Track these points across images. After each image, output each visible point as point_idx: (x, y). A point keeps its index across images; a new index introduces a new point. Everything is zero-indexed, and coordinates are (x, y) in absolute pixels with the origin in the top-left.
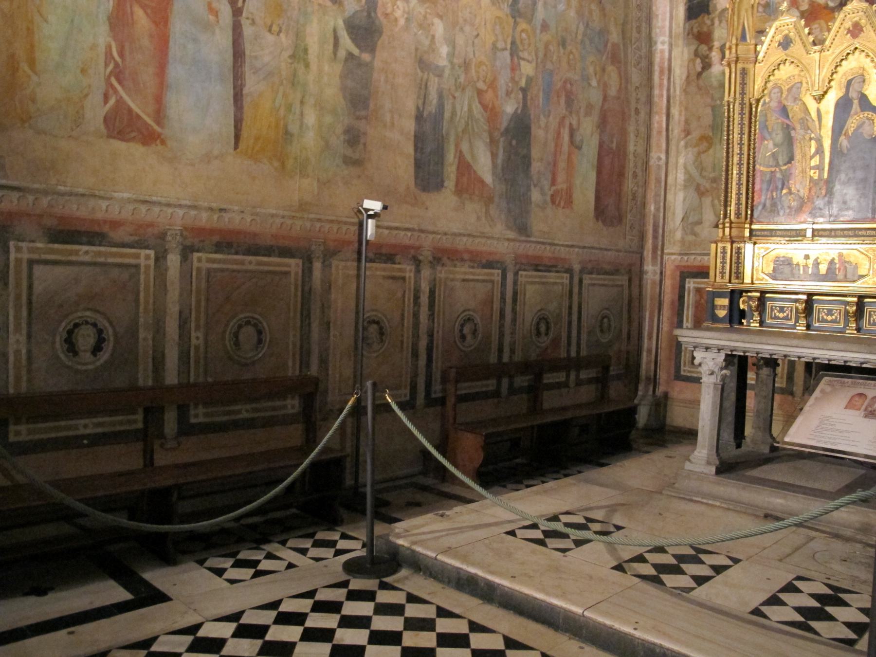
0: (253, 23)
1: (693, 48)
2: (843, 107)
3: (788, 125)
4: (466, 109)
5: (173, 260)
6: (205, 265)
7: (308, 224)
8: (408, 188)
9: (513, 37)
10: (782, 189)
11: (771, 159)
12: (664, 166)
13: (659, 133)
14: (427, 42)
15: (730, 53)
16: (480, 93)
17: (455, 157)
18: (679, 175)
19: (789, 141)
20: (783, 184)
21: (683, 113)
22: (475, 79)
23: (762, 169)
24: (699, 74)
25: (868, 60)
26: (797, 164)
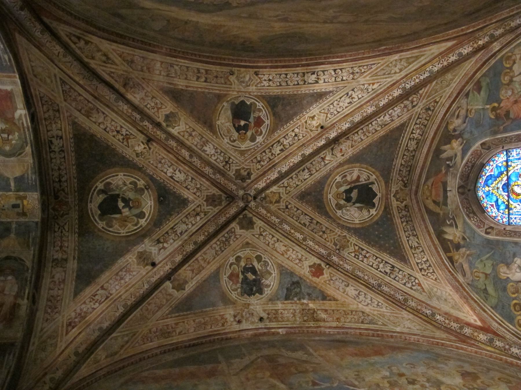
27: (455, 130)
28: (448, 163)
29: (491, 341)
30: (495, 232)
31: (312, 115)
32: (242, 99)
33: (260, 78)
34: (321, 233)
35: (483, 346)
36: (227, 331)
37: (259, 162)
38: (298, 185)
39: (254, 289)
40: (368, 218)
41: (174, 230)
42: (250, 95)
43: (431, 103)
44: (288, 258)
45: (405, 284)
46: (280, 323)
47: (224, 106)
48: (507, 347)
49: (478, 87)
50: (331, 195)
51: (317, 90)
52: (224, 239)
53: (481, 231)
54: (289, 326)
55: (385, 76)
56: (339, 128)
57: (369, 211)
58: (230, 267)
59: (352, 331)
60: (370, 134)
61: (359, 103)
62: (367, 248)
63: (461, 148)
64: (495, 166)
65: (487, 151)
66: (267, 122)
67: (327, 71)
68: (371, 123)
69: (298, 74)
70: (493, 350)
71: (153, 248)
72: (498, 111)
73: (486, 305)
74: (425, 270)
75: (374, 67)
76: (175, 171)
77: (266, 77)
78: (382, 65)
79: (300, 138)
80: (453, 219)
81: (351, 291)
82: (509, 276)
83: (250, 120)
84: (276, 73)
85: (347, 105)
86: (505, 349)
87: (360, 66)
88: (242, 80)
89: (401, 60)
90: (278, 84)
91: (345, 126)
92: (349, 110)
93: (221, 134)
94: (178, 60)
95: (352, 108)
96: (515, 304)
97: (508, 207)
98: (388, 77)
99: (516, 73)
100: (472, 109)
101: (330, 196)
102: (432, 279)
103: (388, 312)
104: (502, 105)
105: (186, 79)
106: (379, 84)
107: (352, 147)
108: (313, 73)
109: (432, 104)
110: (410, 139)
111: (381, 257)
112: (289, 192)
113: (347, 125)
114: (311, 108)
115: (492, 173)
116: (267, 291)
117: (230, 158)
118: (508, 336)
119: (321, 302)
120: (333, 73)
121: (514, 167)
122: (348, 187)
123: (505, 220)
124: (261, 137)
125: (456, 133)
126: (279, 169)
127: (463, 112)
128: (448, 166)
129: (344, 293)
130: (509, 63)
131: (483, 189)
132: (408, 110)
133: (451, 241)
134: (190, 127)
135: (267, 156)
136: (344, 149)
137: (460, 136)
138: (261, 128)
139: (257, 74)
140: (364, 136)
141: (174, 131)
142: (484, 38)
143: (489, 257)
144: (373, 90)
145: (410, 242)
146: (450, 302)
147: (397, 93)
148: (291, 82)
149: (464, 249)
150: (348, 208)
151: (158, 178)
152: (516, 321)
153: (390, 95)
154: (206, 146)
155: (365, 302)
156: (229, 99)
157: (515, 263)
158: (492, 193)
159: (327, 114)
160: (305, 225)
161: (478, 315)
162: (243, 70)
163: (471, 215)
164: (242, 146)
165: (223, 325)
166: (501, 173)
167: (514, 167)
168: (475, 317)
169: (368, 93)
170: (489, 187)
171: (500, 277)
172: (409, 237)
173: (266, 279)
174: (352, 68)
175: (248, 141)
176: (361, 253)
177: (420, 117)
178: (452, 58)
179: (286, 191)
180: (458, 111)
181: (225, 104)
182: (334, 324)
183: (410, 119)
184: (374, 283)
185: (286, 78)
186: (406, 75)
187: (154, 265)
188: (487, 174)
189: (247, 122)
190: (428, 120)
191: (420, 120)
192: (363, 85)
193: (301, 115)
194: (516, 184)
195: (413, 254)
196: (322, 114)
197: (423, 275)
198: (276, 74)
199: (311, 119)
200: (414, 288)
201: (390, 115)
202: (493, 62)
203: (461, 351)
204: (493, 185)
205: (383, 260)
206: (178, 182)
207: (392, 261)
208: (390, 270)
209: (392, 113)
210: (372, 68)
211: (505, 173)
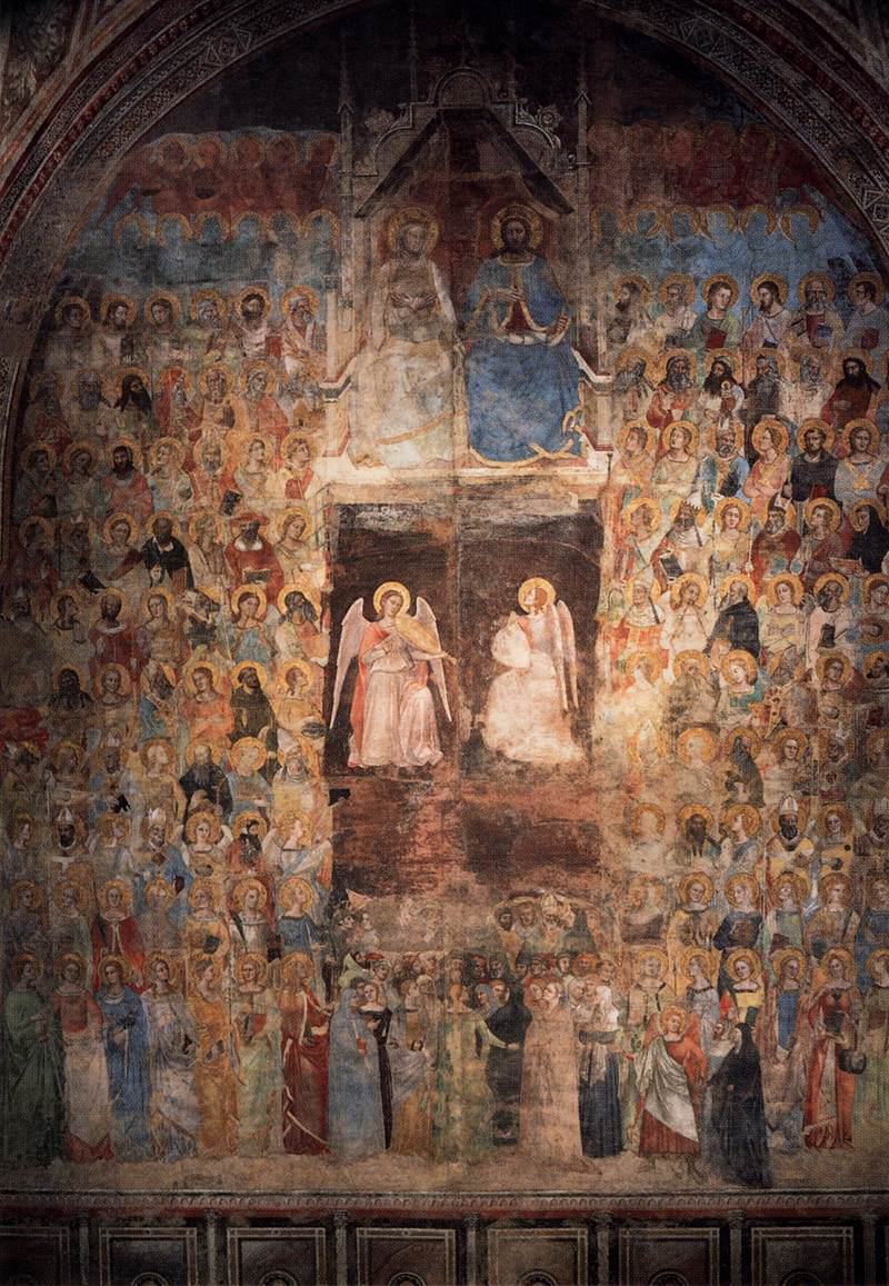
0: (397, 1046)
4: (649, 1066)
5: (341, 1233)
6: (366, 1236)
7: (460, 1201)
8: (574, 1156)
9: (722, 970)
14: (588, 1014)
16: (669, 1046)
17: (636, 1119)
22: (661, 1030)
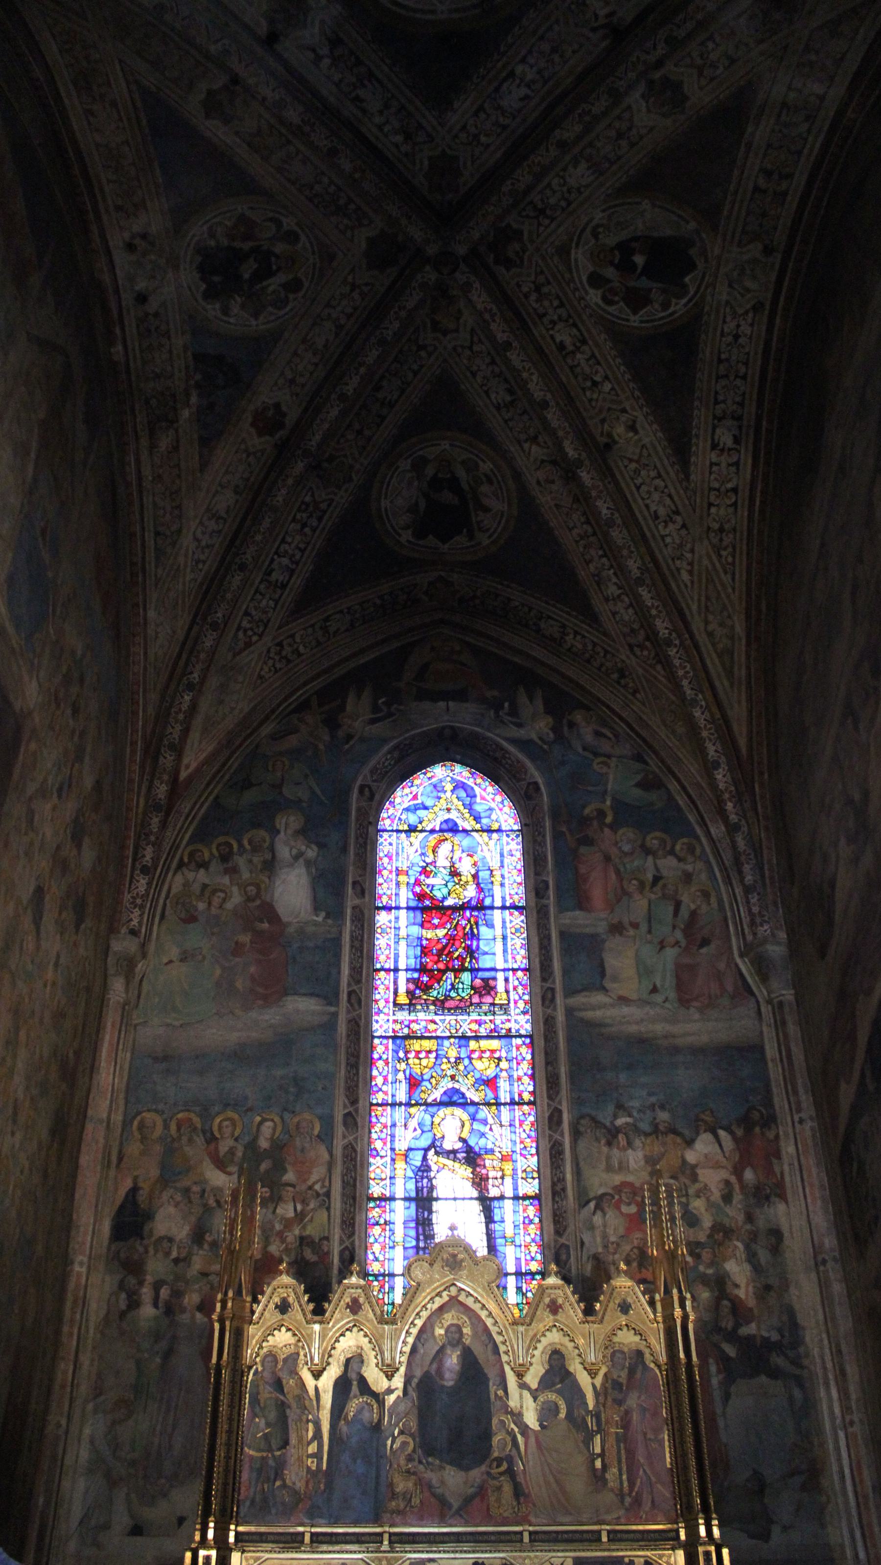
1: (118, 1277)
2: (342, 1386)
3: (283, 1403)
10: (275, 1480)
11: (263, 1443)
12: (63, 1438)
13: (63, 1387)
15: (224, 1307)
18: (81, 1451)
19: (282, 1423)
20: (276, 1474)
21: (96, 1363)
23: (251, 1452)
24: (123, 1315)
25: (367, 1339)
26: (292, 1451)
27: (572, 725)
28: (506, 705)
29: (157, 807)
30: (364, 804)
31: (638, 426)
32: (700, 265)
33: (747, 313)
34: (357, 426)
35: (144, 790)
36: (105, 218)
37: (538, 289)
38: (474, 374)
39: (216, 279)
40: (392, 527)
41: (366, 82)
42: (706, 288)
43: (634, 682)
44: (295, 354)
45: (247, 613)
46: (137, 344)
47: (688, 222)
48: (152, 838)
49: (649, 784)
50: (447, 447)
51: (697, 445)
52: (342, 202)
53: (365, 776)
54: (132, 365)
55: (703, 599)
56: (601, 492)
57: (407, 527)
58: (271, 220)
59: (138, 516)
60: (581, 549)
61: (653, 536)
62: (324, 529)
63: (534, 736)
64: (493, 805)
65: (522, 793)
66: (635, 320)
67: (737, 473)
68: (605, 555)
69: (741, 404)
70: (140, 810)
71: (316, 30)
72: (595, 823)
73: (220, 786)
74: (279, 653)
75: (726, 579)
76: (528, 86)
77: (746, 329)
78: (728, 597)
79: (588, 393)
80: (390, 715)
81: (225, 501)
82: (282, 833)
83: (644, 278)
84: (752, 354)
85: (653, 508)
86: (147, 835)
87: (734, 547)
88: (748, 272)
89: (732, 638)
90: (723, 356)
91: (604, 508)
92: (641, 512)
93: (616, 206)
94: (822, 136)
95: (645, 519)
96: (230, 846)
97: (412, 829)
98: (699, 606)
99: (661, 863)
100: (608, 766)
101: (445, 445)
102: (262, 669)
103: (184, 584)
104: (607, 830)
105: (769, 146)
106: (689, 584)
107: (556, 505)
108: (737, 440)
109: (631, 685)
110: (564, 626)
111: (304, 559)
112: (459, 355)
113: (604, 511)
114: (655, 426)
115: (478, 799)
116: (214, 309)
117: (553, 219)
118: (170, 835)
119: (196, 436)
120: (729, 486)
121: (487, 844)
122: (465, 486)
123: (387, 822)
124: (600, 302)
125: (566, 729)
126: (515, 344)
127: (605, 747)
128: (498, 707)
129: (220, 485)
130: (682, 849)
131: (449, 779)
132: (624, 636)
133: (342, 708)
134: (641, 137)
135: (550, 311)
136: (554, 487)
137: (560, 737)
138: (622, 304)
139: (757, 308)
140: (579, 535)
141: (635, 98)
142: (737, 814)
143: (313, 793)
144: (678, 570)
145: (338, 616)
146: (217, 711)
147: (662, 627)
148: (723, 387)
149: (327, 738)
150: (416, 483)
151: (510, 40)
152: (199, 846)
153: (660, 612)
154: (589, 168)
155: (204, 533)
156: (704, 236)
157: (307, 846)
158: (439, 798)
159: (637, 462)
160: (378, 388)
161: (198, 770)
162: (773, 277)
163: (396, 754)
164: (580, 251)
165: (118, 208)
166: (477, 819)
167: (487, 844)
168: (194, 765)
169: (673, 559)
170: (453, 791)
171: (279, 817)
172: (348, 613)
173: (243, 307)
174: (734, 530)
175: (591, 269)
176: (311, 516)
177: (608, 656)
178: (714, 748)
179: (462, 347)
180: (611, 736)
181: (693, 225)
182: (147, 472)
183: (605, 634)
184: (248, 556)
185: (737, 376)
186: (696, 646)
187: (271, 39)
188: (476, 788)
189: (639, 271)
190: (599, 669)
191: (602, 654)
192: (692, 551)
193: (642, 401)
194: (456, 847)
195: (312, 626)
196: (638, 451)
197: (269, 651)
198: (748, 354)
199: (630, 423)
200: (241, 634)
201: (619, 596)
202: (692, 818)
203: (128, 750)
204: (455, 801)
205: (297, 563)
206: (497, 90)
207: (297, 582)
208: (277, 581)
209: (622, 601)
210: (726, 573)
211: (478, 827)
